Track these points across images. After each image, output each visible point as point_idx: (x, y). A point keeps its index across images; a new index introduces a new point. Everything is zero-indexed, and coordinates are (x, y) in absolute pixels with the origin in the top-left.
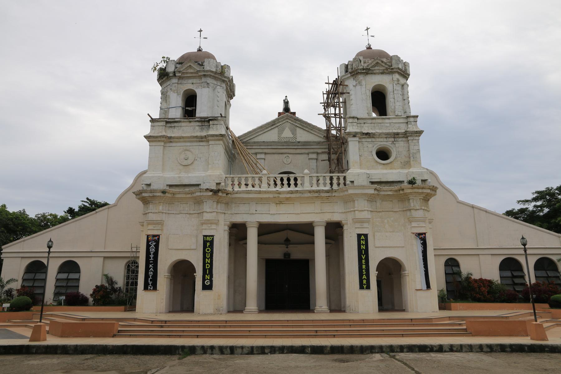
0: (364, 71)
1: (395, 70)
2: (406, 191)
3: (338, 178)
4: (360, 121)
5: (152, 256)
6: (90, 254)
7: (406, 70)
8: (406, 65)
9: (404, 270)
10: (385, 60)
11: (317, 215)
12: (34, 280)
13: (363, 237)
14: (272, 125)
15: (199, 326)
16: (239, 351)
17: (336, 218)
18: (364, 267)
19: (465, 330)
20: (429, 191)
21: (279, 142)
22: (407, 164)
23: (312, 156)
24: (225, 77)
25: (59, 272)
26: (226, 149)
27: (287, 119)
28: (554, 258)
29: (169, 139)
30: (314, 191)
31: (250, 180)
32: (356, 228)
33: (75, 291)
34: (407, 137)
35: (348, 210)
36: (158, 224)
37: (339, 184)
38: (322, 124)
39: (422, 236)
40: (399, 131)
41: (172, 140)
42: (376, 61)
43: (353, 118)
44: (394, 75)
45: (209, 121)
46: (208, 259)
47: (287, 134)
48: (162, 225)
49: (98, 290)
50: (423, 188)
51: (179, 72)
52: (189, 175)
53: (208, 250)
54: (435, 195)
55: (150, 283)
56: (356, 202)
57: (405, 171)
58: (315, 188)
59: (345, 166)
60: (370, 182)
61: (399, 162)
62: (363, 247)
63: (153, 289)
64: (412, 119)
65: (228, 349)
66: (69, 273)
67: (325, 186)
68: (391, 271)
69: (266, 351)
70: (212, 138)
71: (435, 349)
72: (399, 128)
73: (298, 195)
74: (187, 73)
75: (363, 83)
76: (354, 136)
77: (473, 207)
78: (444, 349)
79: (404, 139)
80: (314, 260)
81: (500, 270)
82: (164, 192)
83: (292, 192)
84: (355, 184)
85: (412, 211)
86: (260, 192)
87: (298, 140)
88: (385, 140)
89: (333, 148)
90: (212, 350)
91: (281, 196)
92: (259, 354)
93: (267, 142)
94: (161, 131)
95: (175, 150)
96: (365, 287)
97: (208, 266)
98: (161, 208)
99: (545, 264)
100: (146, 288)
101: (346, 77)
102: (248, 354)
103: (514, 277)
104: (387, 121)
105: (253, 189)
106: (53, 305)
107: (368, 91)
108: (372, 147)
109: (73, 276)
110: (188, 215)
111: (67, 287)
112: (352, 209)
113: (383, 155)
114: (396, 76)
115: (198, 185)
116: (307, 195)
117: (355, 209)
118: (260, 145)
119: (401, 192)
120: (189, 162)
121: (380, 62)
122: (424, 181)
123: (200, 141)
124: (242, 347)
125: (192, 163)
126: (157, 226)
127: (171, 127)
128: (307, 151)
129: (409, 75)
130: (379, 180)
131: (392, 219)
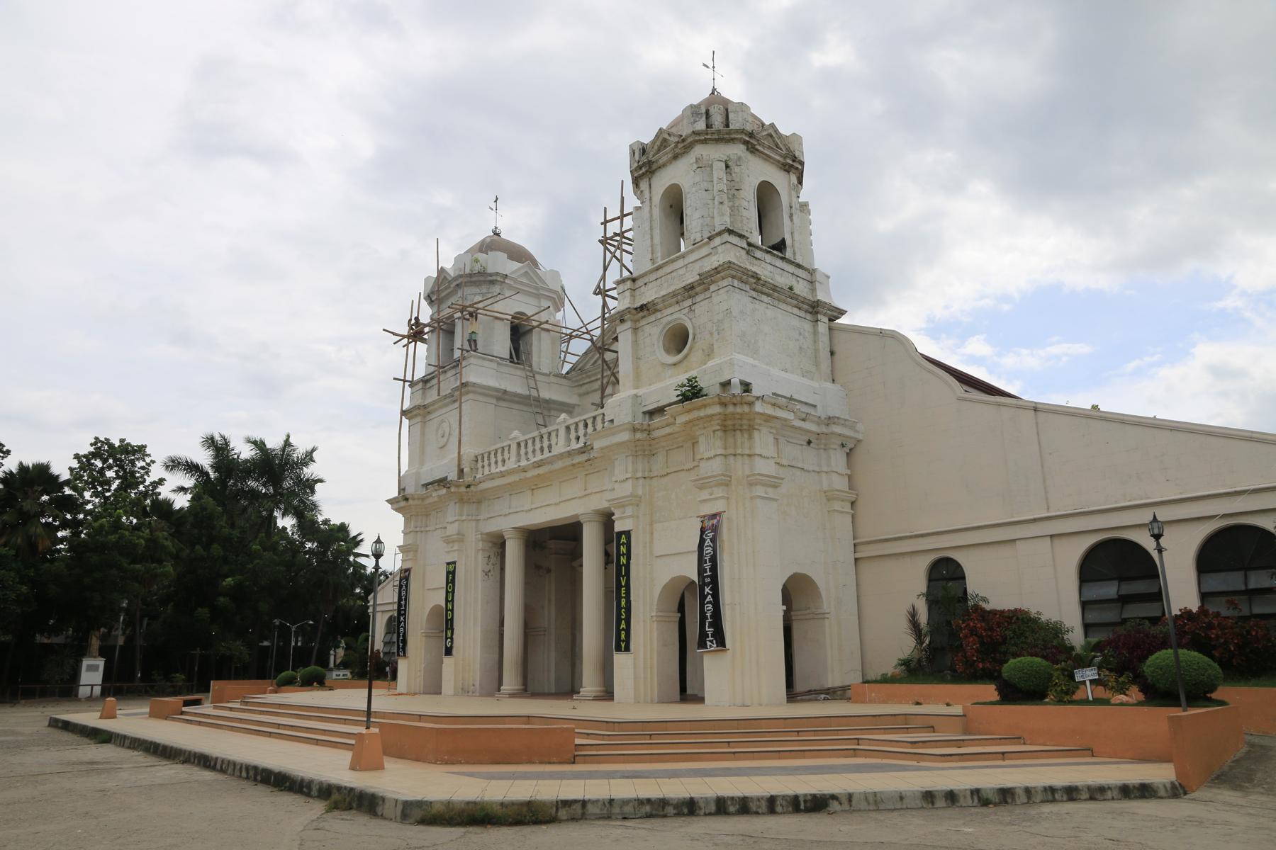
0: (644, 170)
1: (689, 140)
4: (639, 283)
24: (491, 275)
76: (622, 321)
86: (502, 475)
88: (677, 308)
91: (529, 474)
104: (680, 263)
108: (654, 331)
116: (559, 465)
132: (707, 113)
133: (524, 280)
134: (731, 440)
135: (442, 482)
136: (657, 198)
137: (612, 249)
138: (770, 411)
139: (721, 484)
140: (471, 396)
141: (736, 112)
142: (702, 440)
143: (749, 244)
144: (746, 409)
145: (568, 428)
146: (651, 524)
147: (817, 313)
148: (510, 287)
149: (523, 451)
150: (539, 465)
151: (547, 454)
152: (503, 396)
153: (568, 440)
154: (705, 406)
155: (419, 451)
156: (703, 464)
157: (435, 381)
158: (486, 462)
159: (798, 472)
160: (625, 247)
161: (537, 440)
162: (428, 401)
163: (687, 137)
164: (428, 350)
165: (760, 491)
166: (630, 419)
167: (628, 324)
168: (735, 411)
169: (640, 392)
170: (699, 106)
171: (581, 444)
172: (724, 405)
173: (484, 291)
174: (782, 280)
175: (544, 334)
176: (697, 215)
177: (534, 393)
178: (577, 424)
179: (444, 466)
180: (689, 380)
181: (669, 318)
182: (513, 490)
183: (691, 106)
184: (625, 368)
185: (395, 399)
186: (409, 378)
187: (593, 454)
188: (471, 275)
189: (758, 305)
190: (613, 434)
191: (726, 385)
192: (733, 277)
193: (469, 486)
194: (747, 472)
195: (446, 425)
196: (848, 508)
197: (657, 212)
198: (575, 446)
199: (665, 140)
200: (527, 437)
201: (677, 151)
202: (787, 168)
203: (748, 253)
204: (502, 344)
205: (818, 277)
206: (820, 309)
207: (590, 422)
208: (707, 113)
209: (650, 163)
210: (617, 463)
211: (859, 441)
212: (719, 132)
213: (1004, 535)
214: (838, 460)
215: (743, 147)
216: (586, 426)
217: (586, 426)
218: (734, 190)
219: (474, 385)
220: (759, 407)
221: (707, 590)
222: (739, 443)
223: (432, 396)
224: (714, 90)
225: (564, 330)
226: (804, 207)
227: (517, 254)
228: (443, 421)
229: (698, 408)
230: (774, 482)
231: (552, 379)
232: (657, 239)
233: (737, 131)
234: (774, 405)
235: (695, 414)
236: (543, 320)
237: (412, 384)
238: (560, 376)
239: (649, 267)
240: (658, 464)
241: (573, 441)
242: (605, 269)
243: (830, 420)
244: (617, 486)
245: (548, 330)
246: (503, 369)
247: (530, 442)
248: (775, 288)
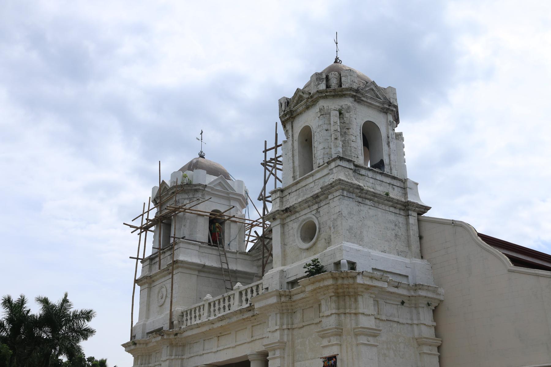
0: (288, 116)
1: (315, 97)
4: (286, 193)
24: (195, 185)
61: (323, 240)
76: (274, 219)
84: (270, 290)
86: (198, 326)
88: (308, 210)
91: (215, 326)
132: (327, 77)
133: (219, 188)
134: (342, 303)
135: (159, 331)
136: (296, 136)
137: (270, 168)
138: (368, 282)
139: (336, 335)
140: (180, 270)
141: (346, 76)
142: (323, 302)
143: (356, 166)
144: (351, 281)
145: (241, 293)
146: (293, 363)
147: (408, 210)
148: (209, 193)
149: (212, 309)
150: (222, 319)
151: (227, 312)
152: (202, 269)
153: (241, 301)
154: (323, 279)
155: (147, 308)
156: (324, 320)
157: (157, 259)
158: (189, 317)
159: (395, 325)
160: (278, 166)
161: (222, 301)
162: (153, 272)
163: (314, 95)
164: (154, 237)
165: (363, 339)
166: (278, 288)
167: (278, 222)
168: (341, 283)
169: (285, 268)
170: (321, 74)
171: (248, 305)
172: (335, 278)
173: (191, 196)
174: (380, 189)
175: (233, 225)
176: (321, 147)
177: (225, 266)
178: (246, 290)
179: (160, 320)
180: (313, 261)
181: (304, 217)
182: (206, 337)
183: (316, 74)
184: (276, 250)
185: (131, 270)
186: (141, 256)
187: (256, 312)
188: (181, 186)
189: (362, 207)
190: (267, 298)
191: (338, 264)
192: (343, 189)
193: (176, 334)
194: (354, 326)
195: (164, 290)
196: (435, 351)
197: (296, 144)
198: (245, 306)
199: (301, 97)
200: (215, 299)
201: (308, 104)
202: (385, 111)
203: (355, 171)
204: (202, 232)
205: (409, 184)
206: (410, 207)
207: (254, 289)
208: (327, 77)
209: (291, 112)
210: (270, 318)
211: (441, 301)
212: (334, 90)
214: (426, 316)
215: (351, 99)
216: (252, 291)
217: (252, 291)
218: (345, 130)
219: (182, 262)
220: (359, 280)
222: (348, 304)
223: (156, 269)
224: (337, 59)
225: (247, 222)
226: (399, 136)
227: (213, 171)
228: (162, 287)
229: (319, 281)
230: (374, 333)
231: (238, 256)
232: (297, 163)
233: (347, 89)
234: (371, 278)
235: (317, 285)
236: (232, 215)
237: (143, 261)
238: (245, 253)
239: (291, 182)
240: (298, 319)
241: (244, 302)
242: (265, 182)
243: (417, 287)
244: (270, 335)
245: (235, 222)
246: (202, 250)
247: (217, 303)
248: (375, 195)
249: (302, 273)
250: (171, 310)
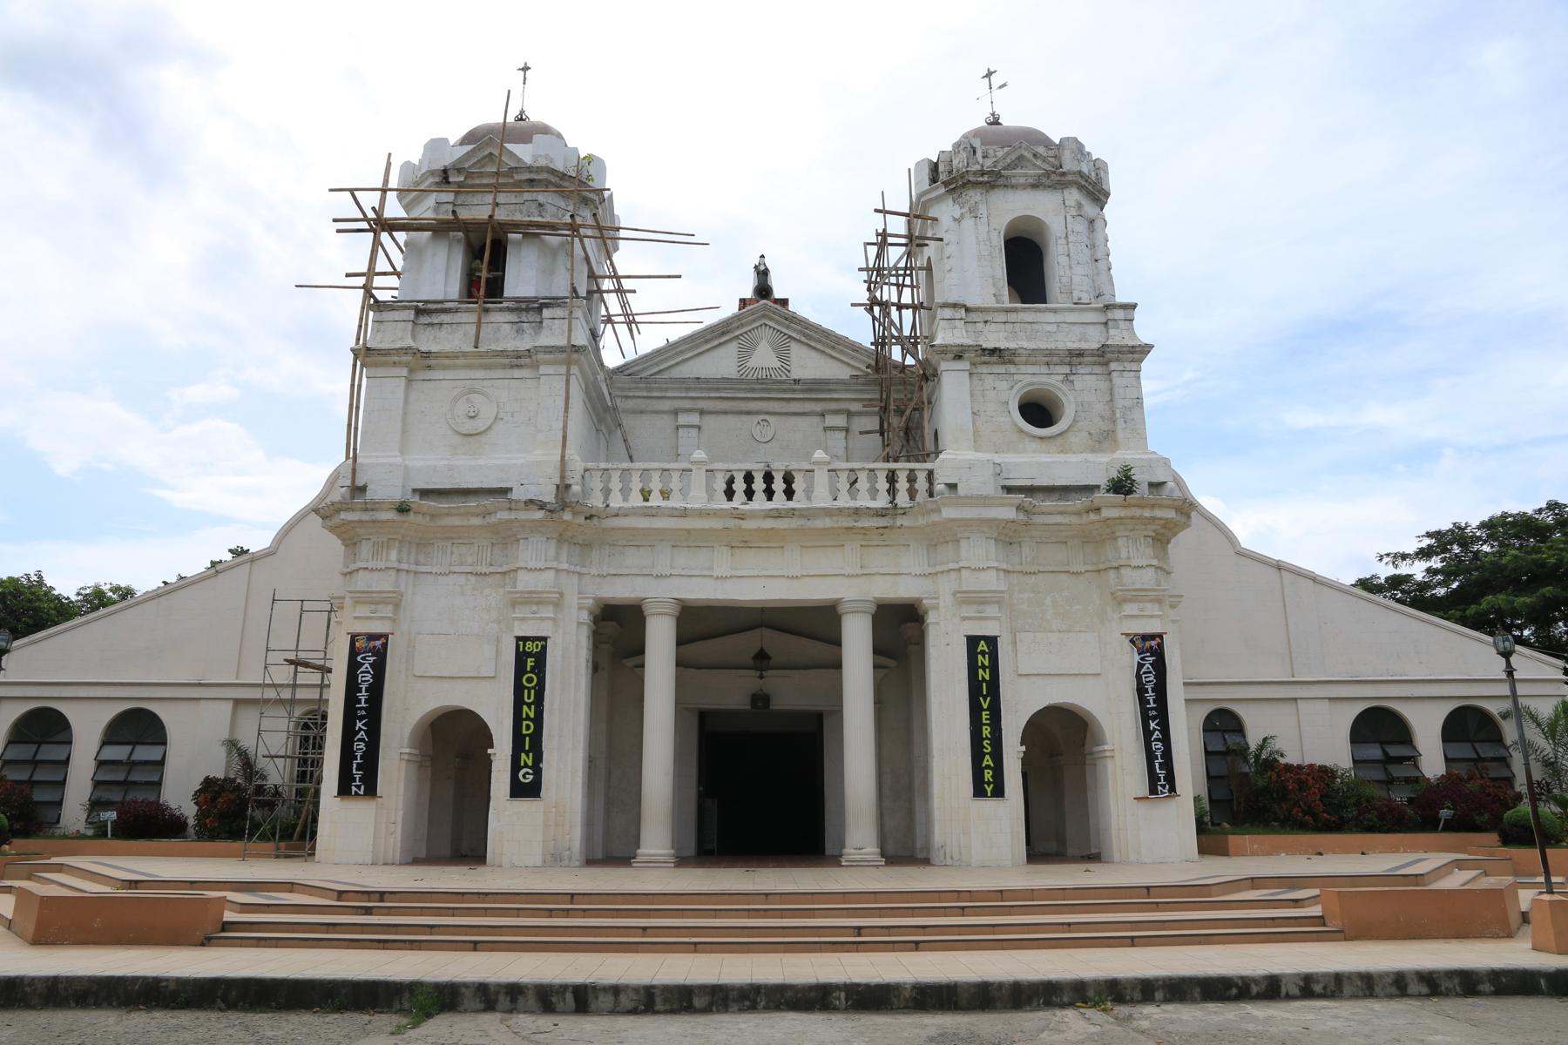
0: (986, 178)
1: (1070, 178)
2: (1106, 513)
3: (912, 479)
4: (974, 316)
5: (363, 696)
6: (194, 692)
7: (1099, 179)
8: (1100, 166)
9: (1099, 740)
10: (1041, 150)
11: (849, 581)
12: (35, 763)
13: (982, 646)
14: (720, 333)
15: (486, 912)
16: (606, 1001)
17: (902, 590)
18: (986, 731)
19: (1321, 920)
20: (1171, 514)
21: (740, 381)
22: (1105, 439)
23: (832, 421)
25: (106, 742)
26: (587, 392)
27: (764, 316)
28: (1494, 708)
29: (422, 361)
30: (840, 510)
31: (656, 476)
32: (964, 619)
33: (152, 798)
34: (1107, 364)
35: (939, 569)
36: (384, 602)
37: (912, 493)
38: (861, 331)
39: (1153, 643)
40: (1084, 346)
41: (432, 362)
42: (1018, 153)
43: (955, 306)
44: (1066, 192)
45: (539, 310)
46: (529, 705)
47: (764, 358)
48: (397, 606)
49: (210, 790)
50: (1153, 506)
51: (459, 171)
52: (481, 462)
53: (530, 680)
54: (1186, 526)
55: (358, 774)
56: (963, 543)
57: (1103, 458)
58: (844, 502)
59: (929, 445)
60: (1003, 487)
61: (1085, 434)
62: (984, 675)
63: (366, 794)
64: (1119, 314)
65: (569, 997)
66: (135, 744)
67: (874, 498)
68: (1062, 740)
69: (697, 1002)
70: (547, 356)
71: (1254, 989)
72: (1083, 338)
73: (795, 523)
74: (481, 175)
75: (983, 209)
76: (959, 357)
77: (1279, 567)
78: (1283, 991)
79: (1098, 369)
80: (838, 712)
81: (1353, 742)
82: (403, 509)
83: (778, 514)
84: (961, 490)
85: (1123, 571)
86: (684, 513)
87: (795, 375)
88: (1044, 369)
89: (894, 400)
90: (514, 1000)
91: (745, 524)
92: (672, 1012)
93: (707, 381)
94: (398, 335)
95: (441, 390)
96: (989, 789)
97: (528, 728)
98: (393, 555)
99: (1468, 725)
100: (344, 790)
101: (933, 195)
102: (633, 1012)
103: (1389, 760)
104: (1050, 317)
105: (664, 504)
106: (84, 837)
107: (994, 235)
108: (1006, 390)
109: (145, 753)
110: (473, 579)
111: (126, 784)
112: (952, 566)
113: (1038, 412)
114: (1073, 196)
115: (504, 491)
117: (962, 564)
118: (687, 389)
119: (1093, 516)
120: (480, 425)
121: (1030, 156)
122: (1156, 486)
123: (512, 367)
124: (616, 990)
125: (490, 428)
126: (380, 607)
127: (432, 324)
128: (818, 407)
129: (1107, 195)
130: (1028, 483)
131: (1066, 593)
181: (1035, 379)
188: (563, 176)
201: (1044, 180)
213: (1288, 694)
221: (1152, 725)
228: (473, 391)
249: (1103, 481)
250: (563, 457)
